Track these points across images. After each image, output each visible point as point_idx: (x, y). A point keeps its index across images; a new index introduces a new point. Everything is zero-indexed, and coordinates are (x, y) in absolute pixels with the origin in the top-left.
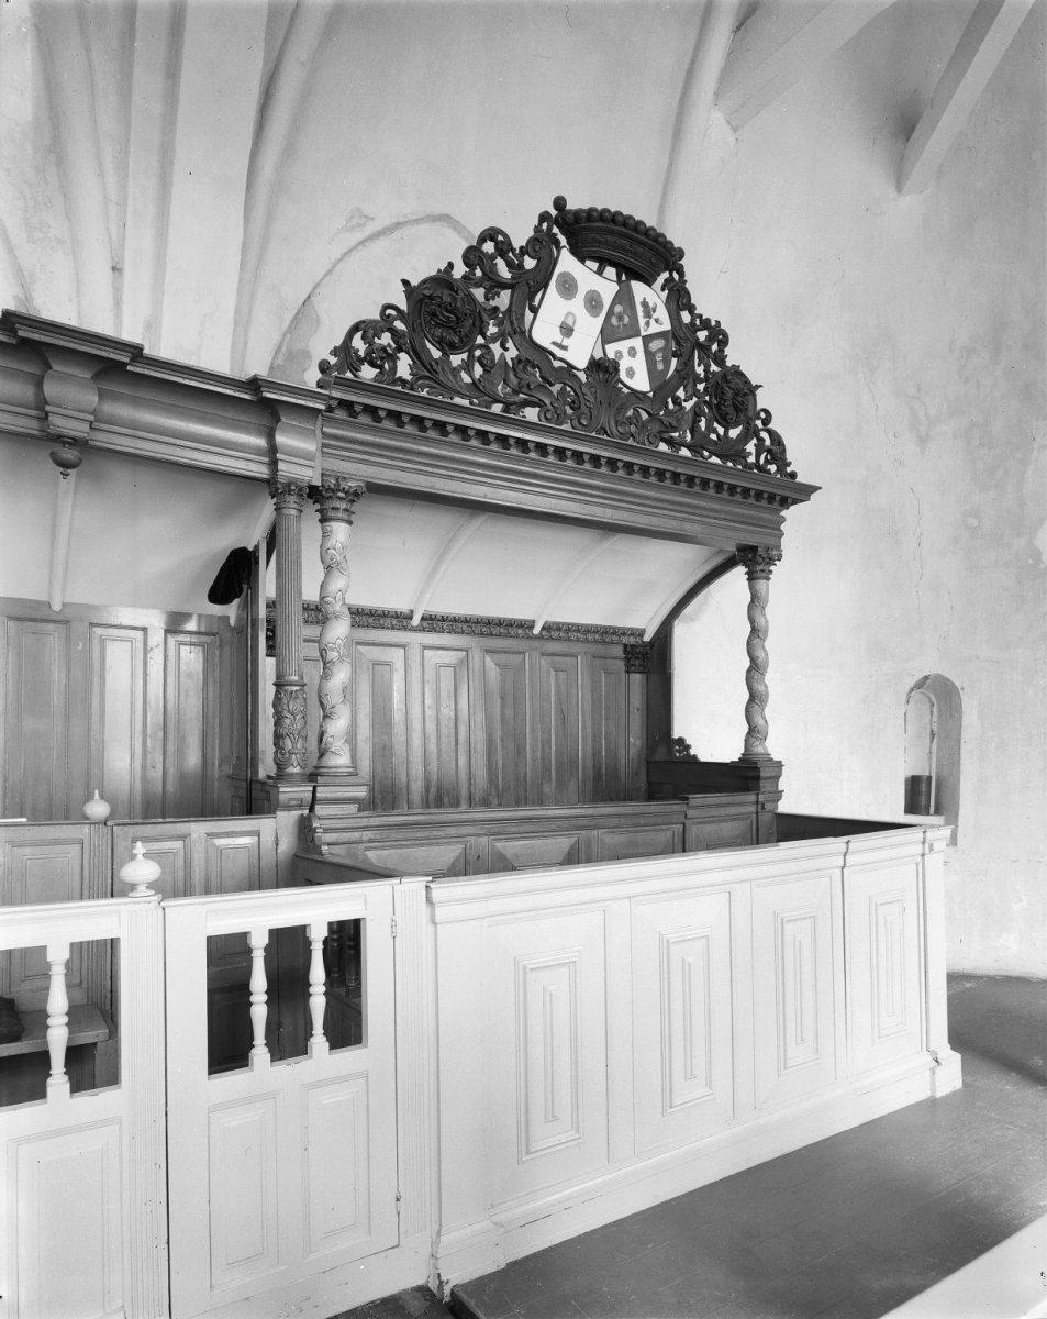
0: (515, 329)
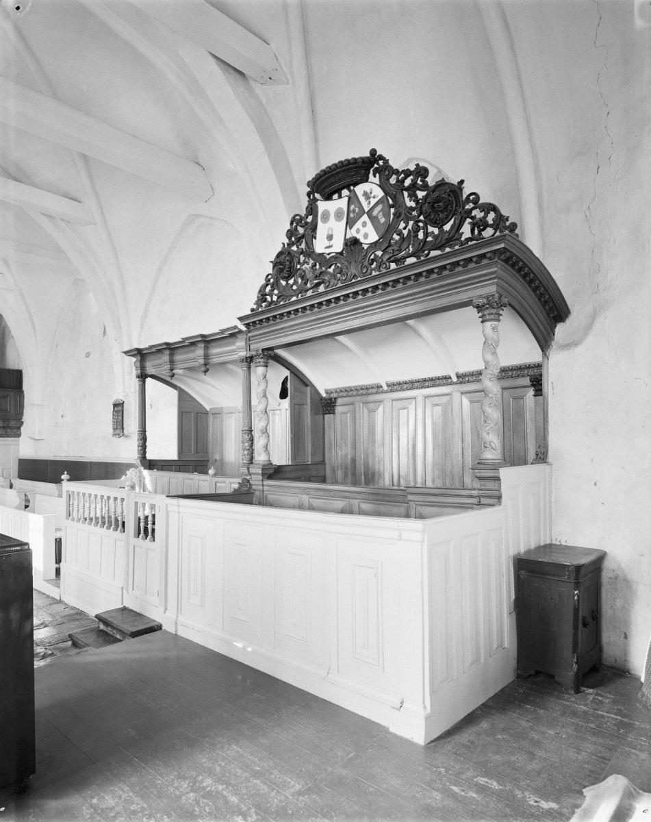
0: (309, 253)
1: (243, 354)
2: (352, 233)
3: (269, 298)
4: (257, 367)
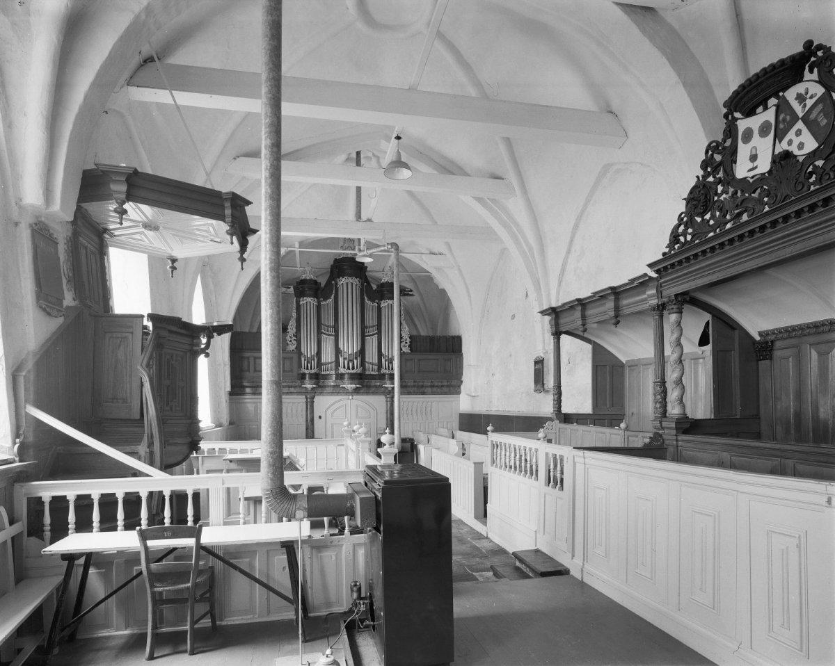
0: (730, 179)
1: (654, 302)
2: (783, 146)
3: (682, 239)
4: (669, 314)
